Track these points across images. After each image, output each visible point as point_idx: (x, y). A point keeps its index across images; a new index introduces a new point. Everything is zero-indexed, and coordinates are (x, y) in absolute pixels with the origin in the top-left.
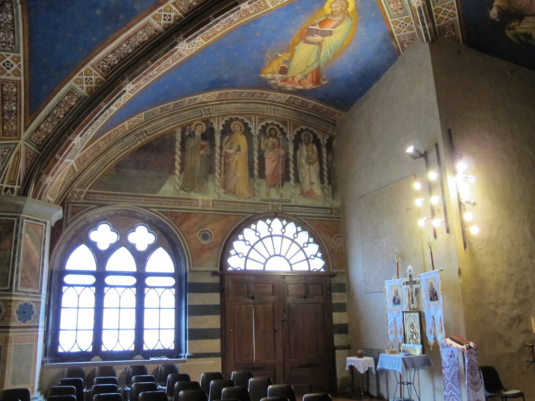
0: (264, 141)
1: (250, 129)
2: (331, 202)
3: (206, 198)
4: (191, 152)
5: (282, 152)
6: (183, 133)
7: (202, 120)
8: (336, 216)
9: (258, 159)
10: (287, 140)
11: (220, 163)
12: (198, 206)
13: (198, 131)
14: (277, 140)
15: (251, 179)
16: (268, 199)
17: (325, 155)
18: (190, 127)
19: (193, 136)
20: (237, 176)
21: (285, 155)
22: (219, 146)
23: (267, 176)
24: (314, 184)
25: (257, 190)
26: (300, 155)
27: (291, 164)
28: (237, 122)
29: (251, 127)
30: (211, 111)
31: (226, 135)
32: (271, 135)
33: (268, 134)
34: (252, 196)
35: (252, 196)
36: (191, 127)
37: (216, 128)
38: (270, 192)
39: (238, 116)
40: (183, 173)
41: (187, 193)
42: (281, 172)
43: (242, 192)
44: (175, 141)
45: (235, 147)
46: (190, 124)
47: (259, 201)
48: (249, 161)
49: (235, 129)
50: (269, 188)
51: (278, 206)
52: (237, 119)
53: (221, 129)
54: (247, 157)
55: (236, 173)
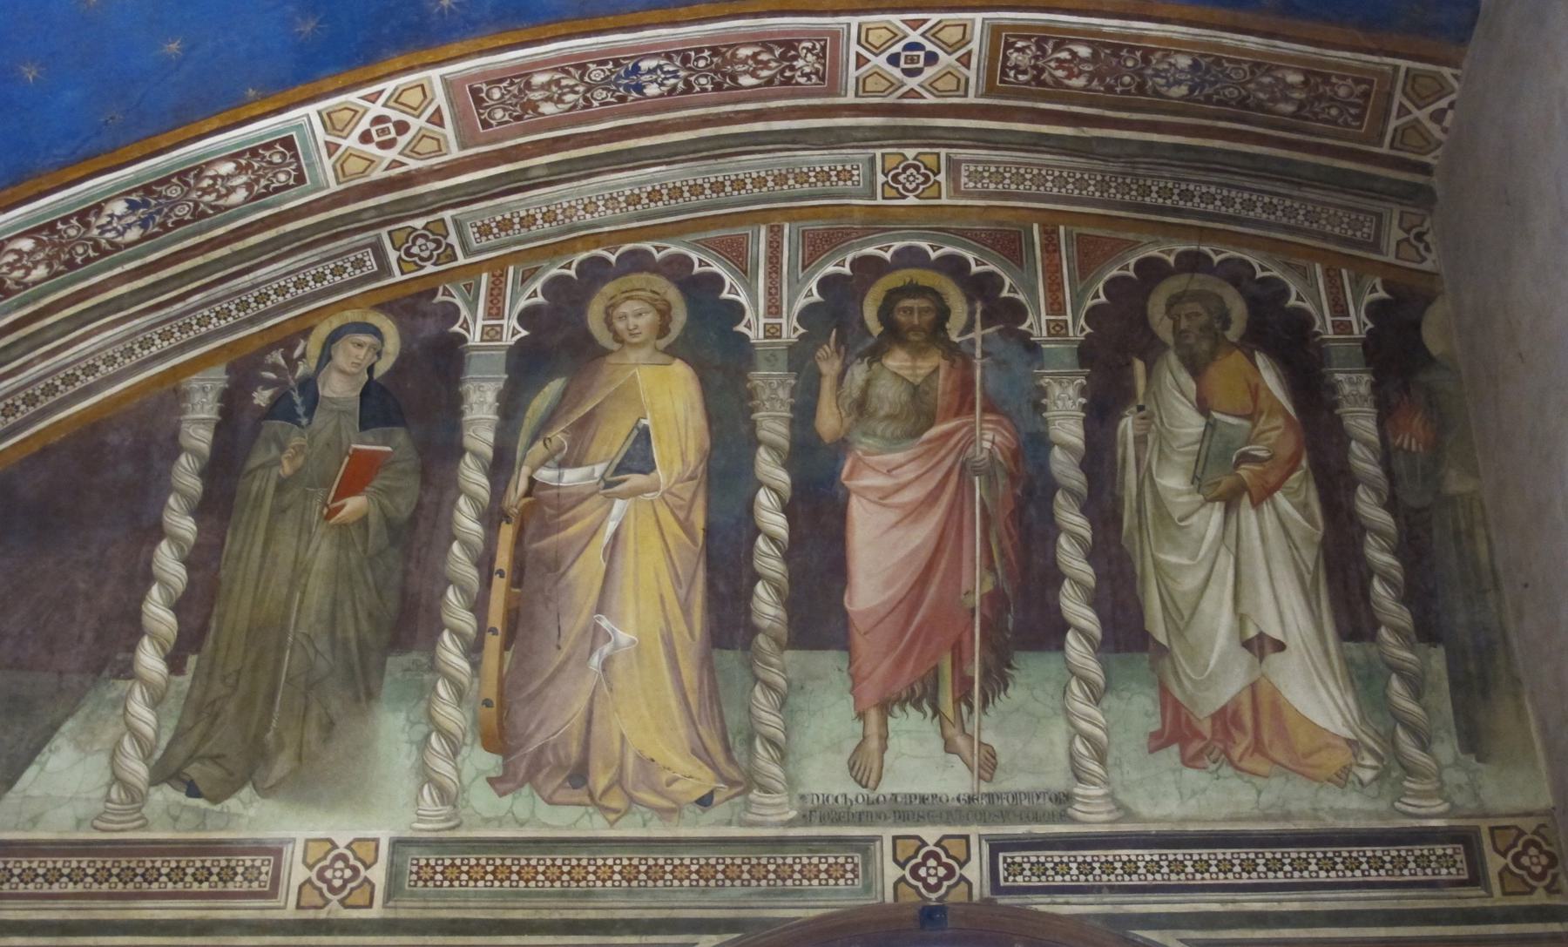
0: (841, 377)
1: (736, 311)
2: (1454, 777)
3: (341, 829)
4: (279, 511)
5: (990, 438)
6: (232, 403)
7: (376, 300)
8: (1524, 901)
9: (788, 509)
10: (1032, 348)
11: (485, 564)
12: (272, 894)
13: (342, 372)
14: (944, 365)
15: (729, 659)
16: (868, 802)
17: (1362, 423)
18: (293, 347)
19: (300, 410)
20: (607, 649)
21: (1016, 455)
22: (489, 452)
23: (859, 625)
24: (1280, 646)
25: (771, 741)
26: (1141, 441)
27: (1072, 519)
28: (638, 279)
29: (743, 299)
30: (453, 239)
31: (550, 376)
32: (894, 334)
33: (875, 327)
34: (731, 783)
35: (724, 790)
36: (297, 353)
37: (474, 338)
38: (884, 748)
39: (648, 246)
40: (192, 660)
41: (201, 803)
42: (977, 584)
43: (646, 763)
44: (174, 449)
45: (612, 441)
46: (287, 340)
47: (790, 823)
48: (708, 532)
49: (620, 325)
50: (873, 716)
51: (957, 848)
52: (637, 262)
53: (509, 340)
54: (700, 502)
55: (605, 623)
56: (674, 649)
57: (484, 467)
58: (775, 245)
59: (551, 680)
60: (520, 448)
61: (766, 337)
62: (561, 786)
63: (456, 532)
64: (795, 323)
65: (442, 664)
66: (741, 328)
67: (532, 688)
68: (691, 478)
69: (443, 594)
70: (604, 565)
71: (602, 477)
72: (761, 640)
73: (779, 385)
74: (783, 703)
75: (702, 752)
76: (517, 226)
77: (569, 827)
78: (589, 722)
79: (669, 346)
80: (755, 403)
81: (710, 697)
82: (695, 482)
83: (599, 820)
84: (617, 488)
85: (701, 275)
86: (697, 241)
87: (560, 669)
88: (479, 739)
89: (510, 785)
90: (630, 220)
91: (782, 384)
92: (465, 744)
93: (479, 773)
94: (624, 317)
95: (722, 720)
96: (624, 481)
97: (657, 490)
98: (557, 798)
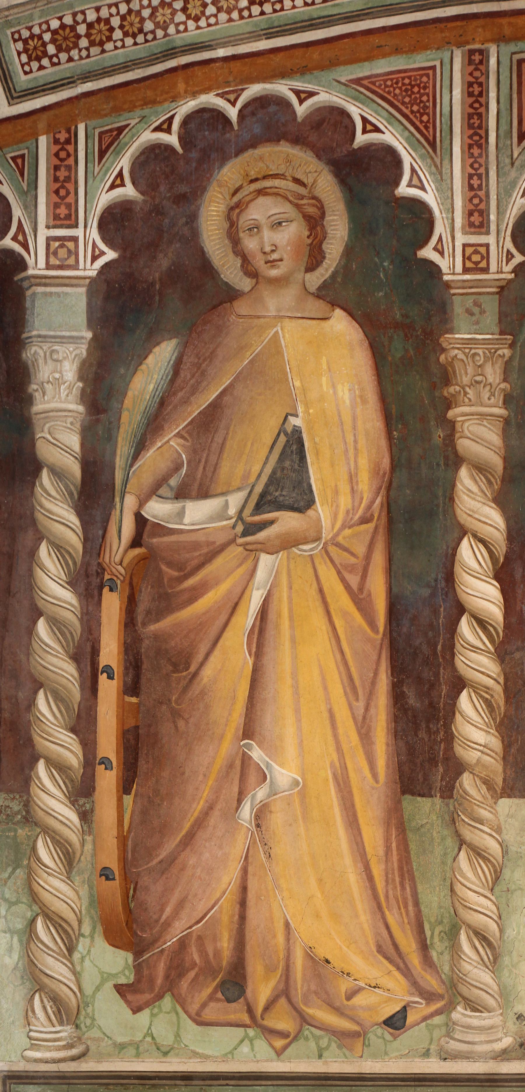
20: (261, 794)
34: (429, 997)
47: (504, 1055)
49: (250, 244)
55: (257, 754)
56: (350, 793)
57: (71, 494)
58: (476, 89)
59: (189, 838)
60: (119, 462)
61: (466, 270)
62: (211, 998)
63: (40, 604)
64: (509, 245)
65: (41, 813)
66: (428, 253)
67: (163, 854)
68: (364, 520)
69: (32, 703)
70: (250, 662)
71: (240, 516)
72: (466, 780)
73: (486, 359)
74: (497, 877)
75: (391, 951)
76: (84, 43)
77: (226, 1057)
78: (243, 903)
79: (324, 286)
80: (452, 389)
81: (401, 868)
82: (371, 526)
83: (262, 1046)
84: (262, 535)
85: (367, 148)
86: (358, 81)
87: (200, 823)
88: (99, 929)
89: (147, 996)
90: (255, 36)
91: (491, 356)
92: (83, 936)
93: (105, 977)
94: (255, 228)
95: (417, 904)
96: (272, 522)
97: (318, 539)
98: (208, 1014)
